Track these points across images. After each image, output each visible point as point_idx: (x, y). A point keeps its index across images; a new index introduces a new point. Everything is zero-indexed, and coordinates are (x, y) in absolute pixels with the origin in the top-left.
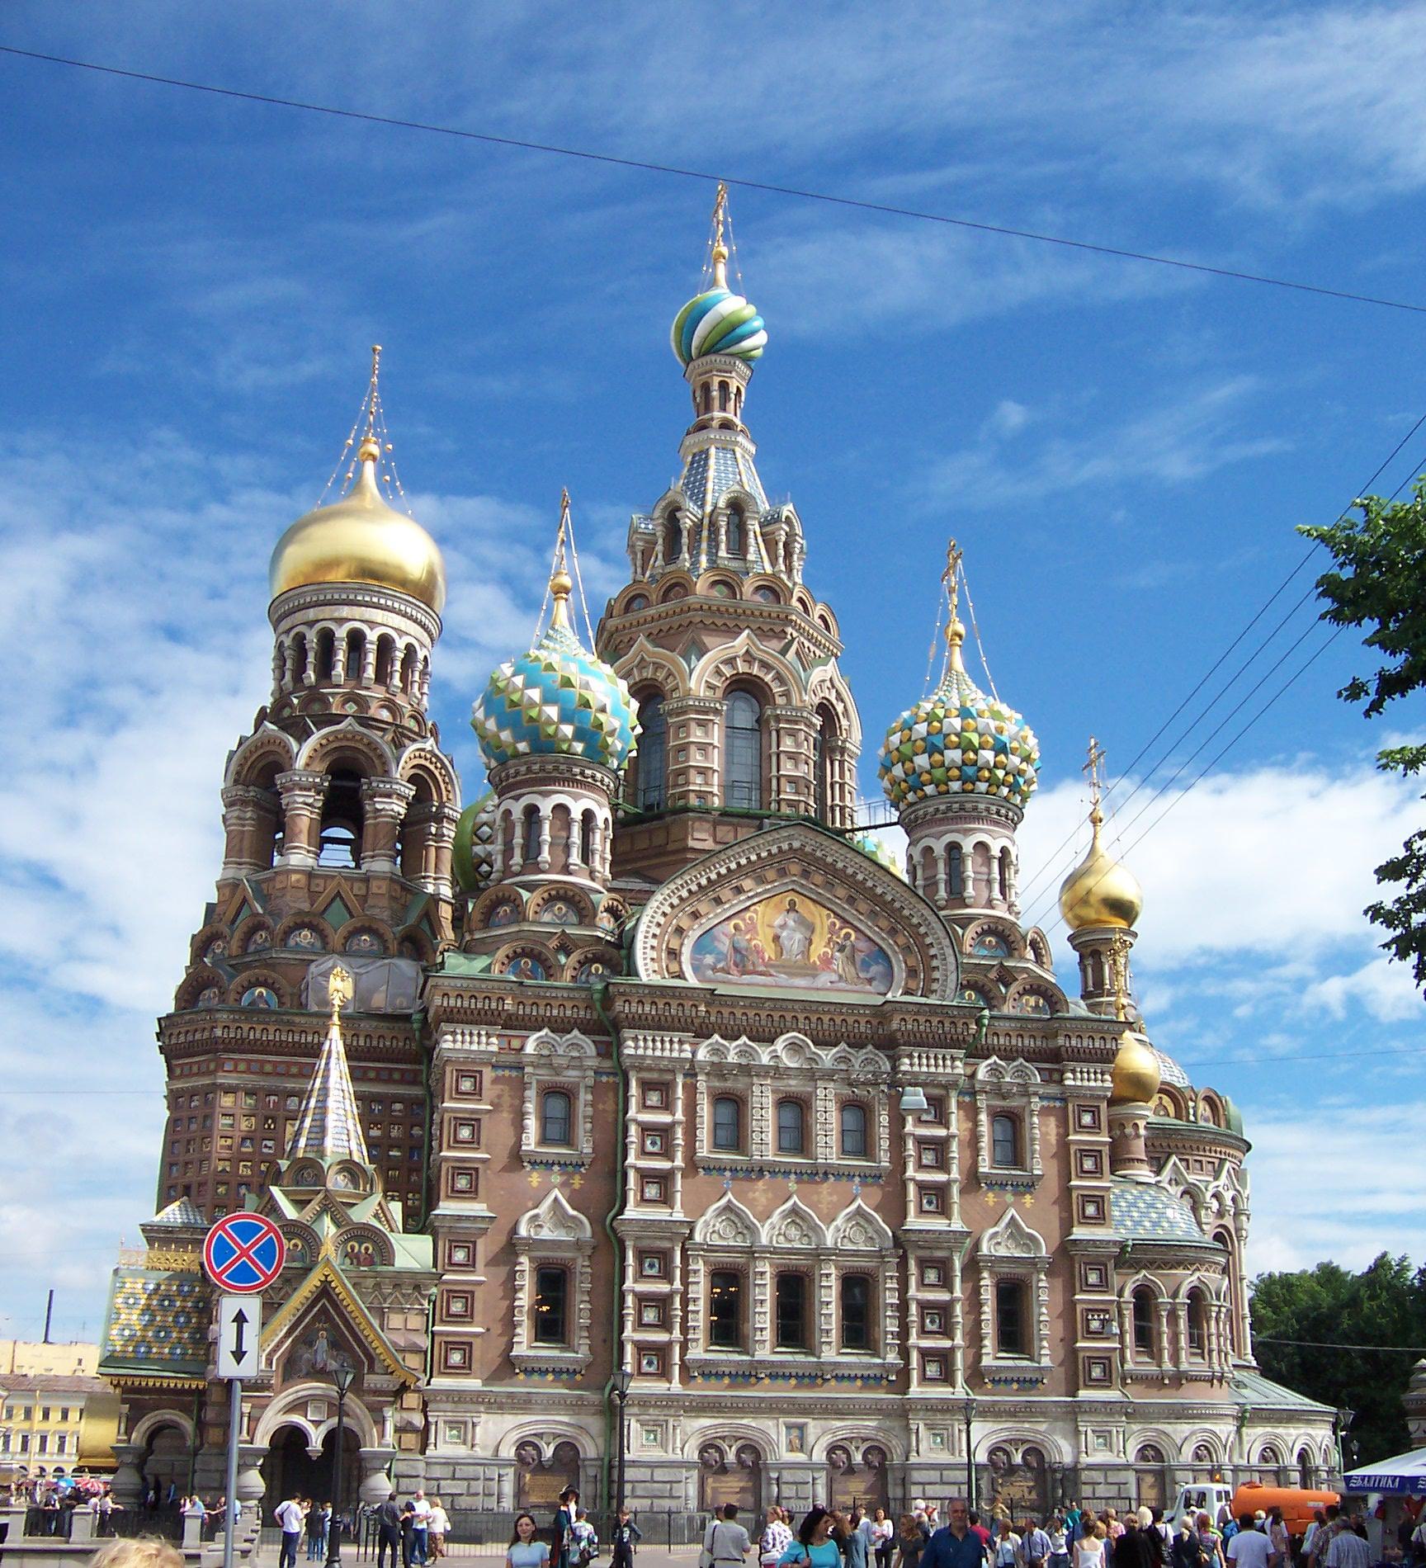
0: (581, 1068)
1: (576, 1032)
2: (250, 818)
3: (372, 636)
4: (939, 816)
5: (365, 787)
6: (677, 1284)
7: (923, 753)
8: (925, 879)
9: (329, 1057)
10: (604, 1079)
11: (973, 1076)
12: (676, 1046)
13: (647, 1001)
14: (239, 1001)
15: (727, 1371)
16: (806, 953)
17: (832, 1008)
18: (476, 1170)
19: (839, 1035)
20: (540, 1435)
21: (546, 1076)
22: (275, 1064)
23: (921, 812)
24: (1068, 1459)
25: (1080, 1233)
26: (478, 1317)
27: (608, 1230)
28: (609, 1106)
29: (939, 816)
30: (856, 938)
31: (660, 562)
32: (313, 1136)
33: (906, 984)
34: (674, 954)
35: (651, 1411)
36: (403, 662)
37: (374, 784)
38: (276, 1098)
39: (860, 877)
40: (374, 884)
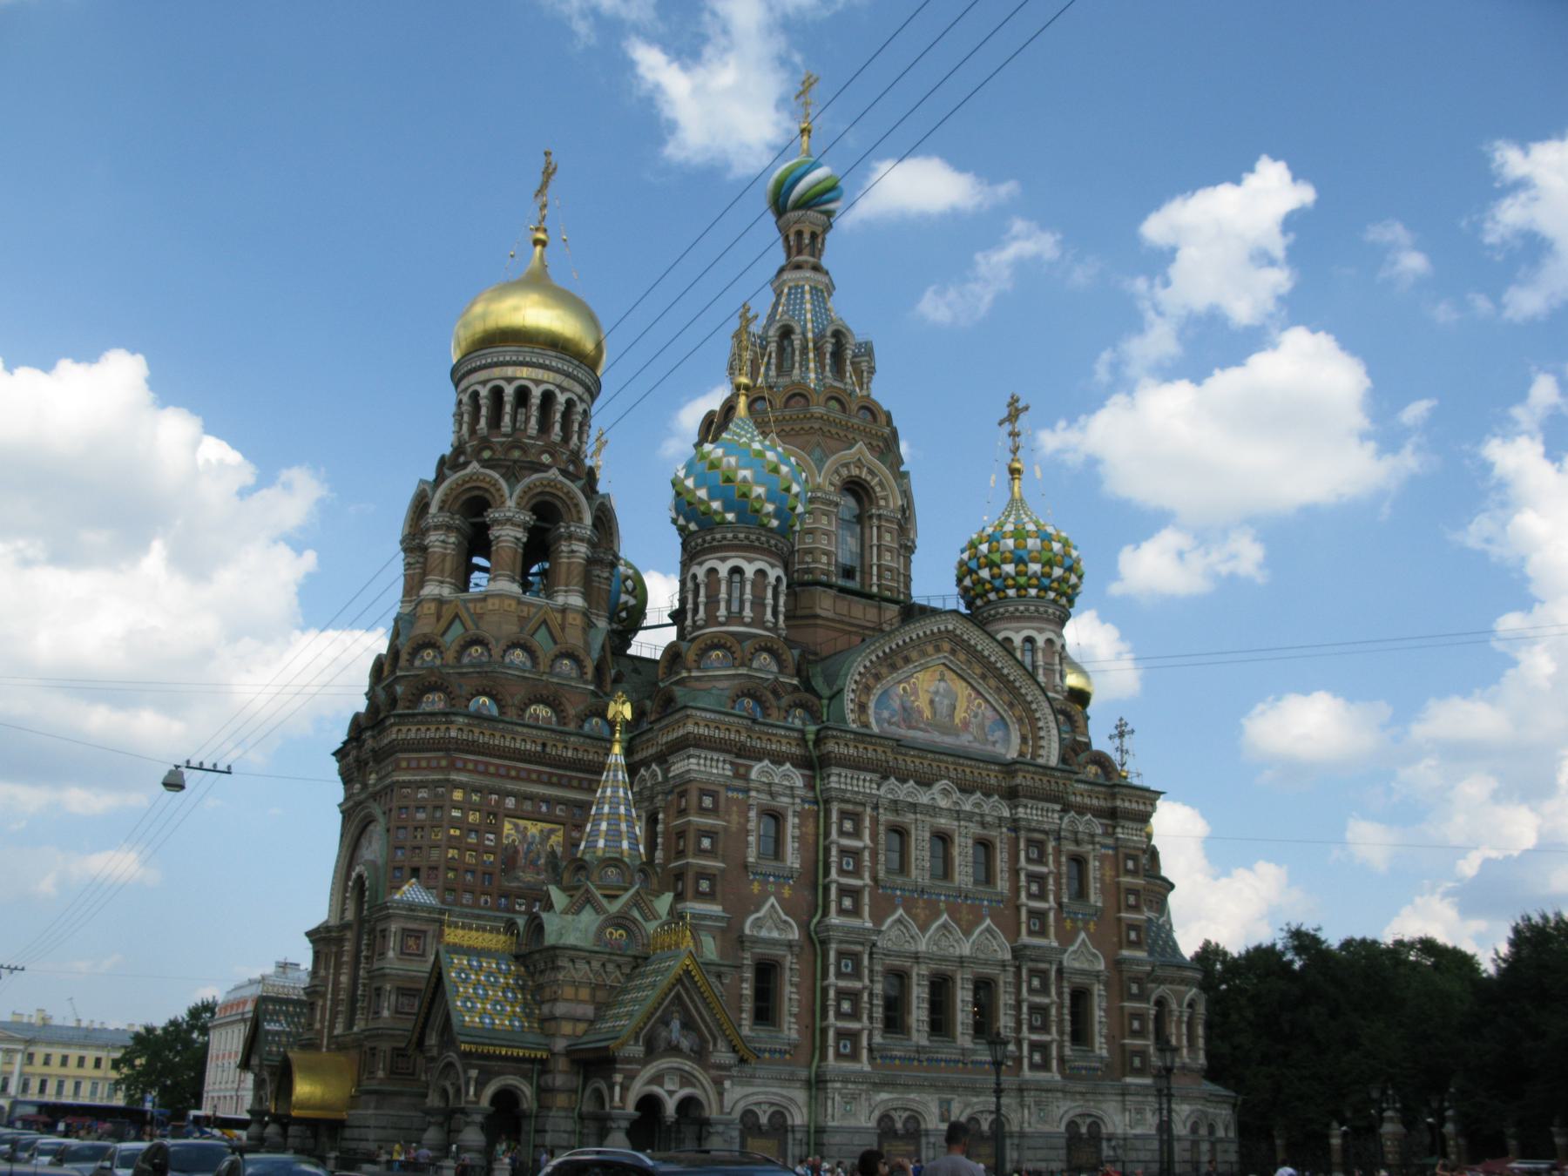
0: (793, 797)
1: (788, 765)
2: (454, 543)
3: (561, 398)
4: (1018, 614)
5: (562, 530)
6: (867, 981)
7: (1011, 562)
9: (616, 771)
10: (806, 806)
12: (867, 784)
13: (851, 744)
14: (467, 707)
15: (898, 1054)
16: (951, 715)
17: (973, 763)
18: (714, 875)
20: (759, 1104)
21: (765, 798)
22: (498, 766)
24: (1119, 1131)
25: (1126, 953)
28: (810, 829)
31: (773, 373)
32: (610, 838)
34: (862, 708)
35: (850, 1086)
36: (581, 425)
37: (573, 529)
38: (496, 797)
40: (570, 617)
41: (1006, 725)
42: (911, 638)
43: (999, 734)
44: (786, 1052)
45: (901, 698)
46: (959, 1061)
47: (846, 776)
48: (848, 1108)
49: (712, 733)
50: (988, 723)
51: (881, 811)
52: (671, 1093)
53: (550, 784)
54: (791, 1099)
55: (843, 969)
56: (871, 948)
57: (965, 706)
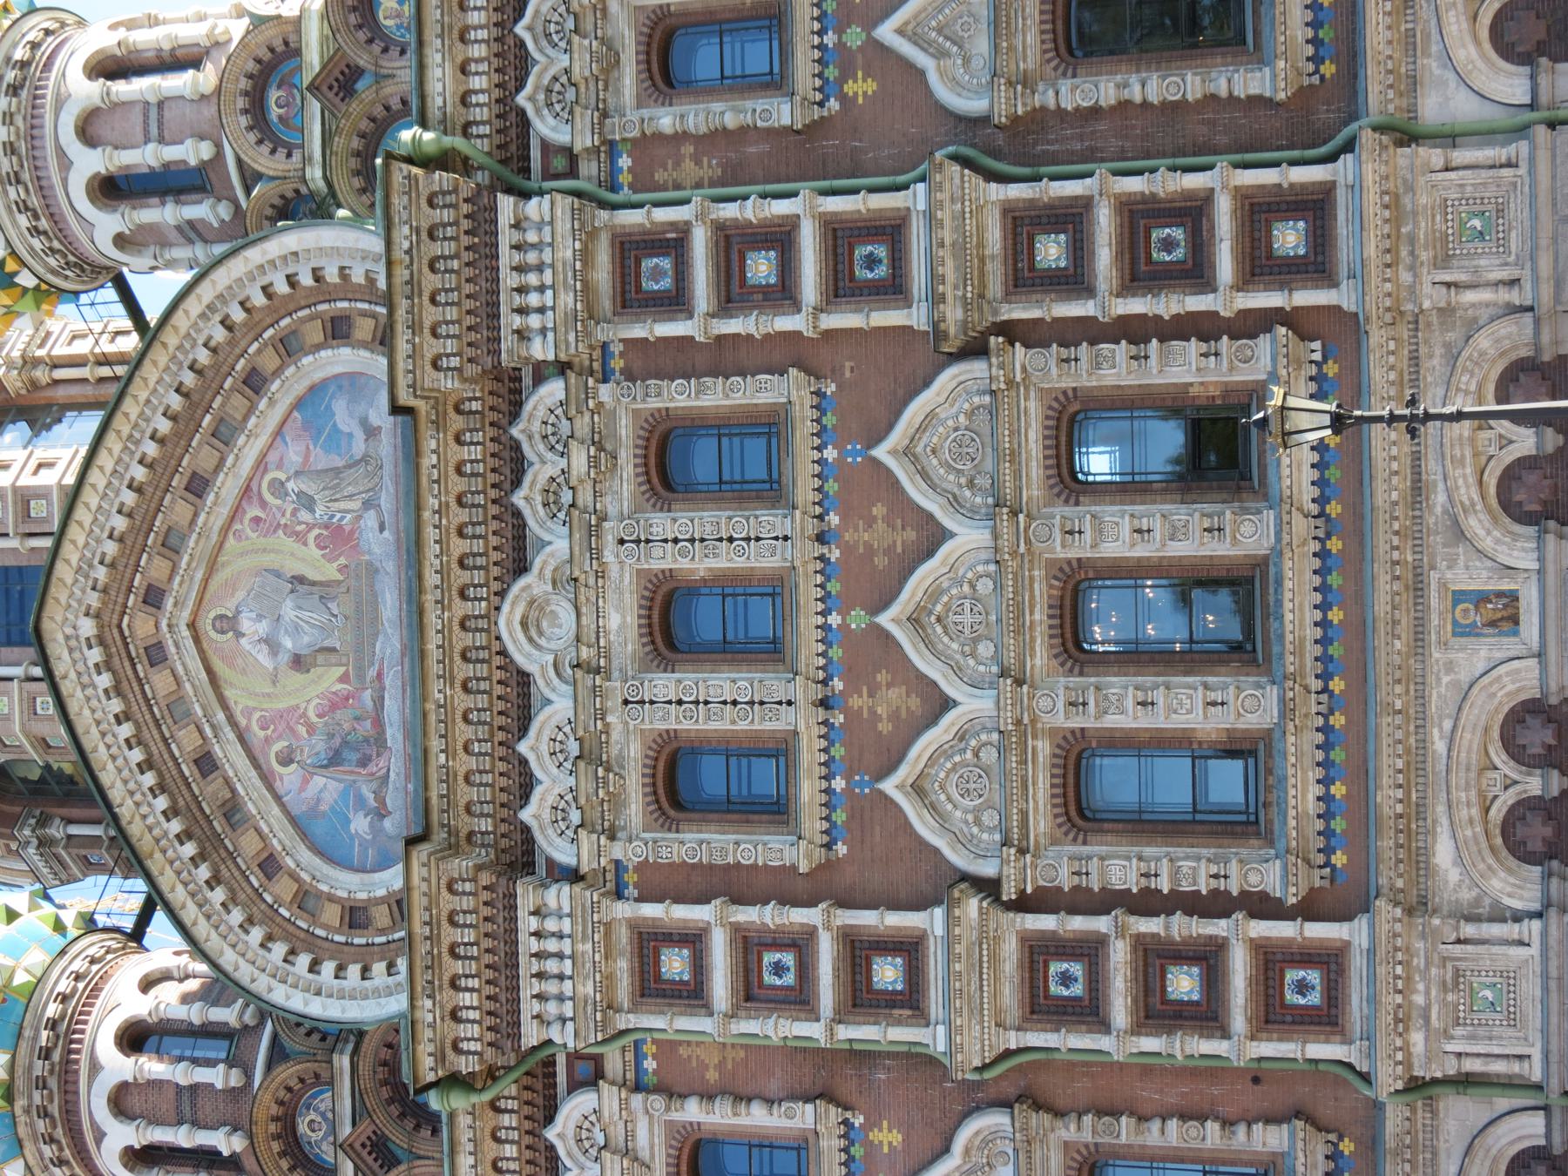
1: (551, 1134)
4: (44, 224)
6: (1102, 924)
8: (191, 242)
10: (650, 1064)
11: (569, 152)
12: (551, 925)
17: (431, 534)
19: (494, 510)
23: (52, 261)
27: (987, 1075)
29: (44, 224)
30: (279, 467)
33: (364, 345)
34: (355, 916)
35: (1419, 999)
39: (140, 473)
41: (312, 389)
42: (145, 766)
43: (343, 415)
45: (309, 772)
47: (540, 997)
48: (1488, 994)
50: (321, 460)
51: (617, 851)
55: (1077, 990)
57: (289, 543)
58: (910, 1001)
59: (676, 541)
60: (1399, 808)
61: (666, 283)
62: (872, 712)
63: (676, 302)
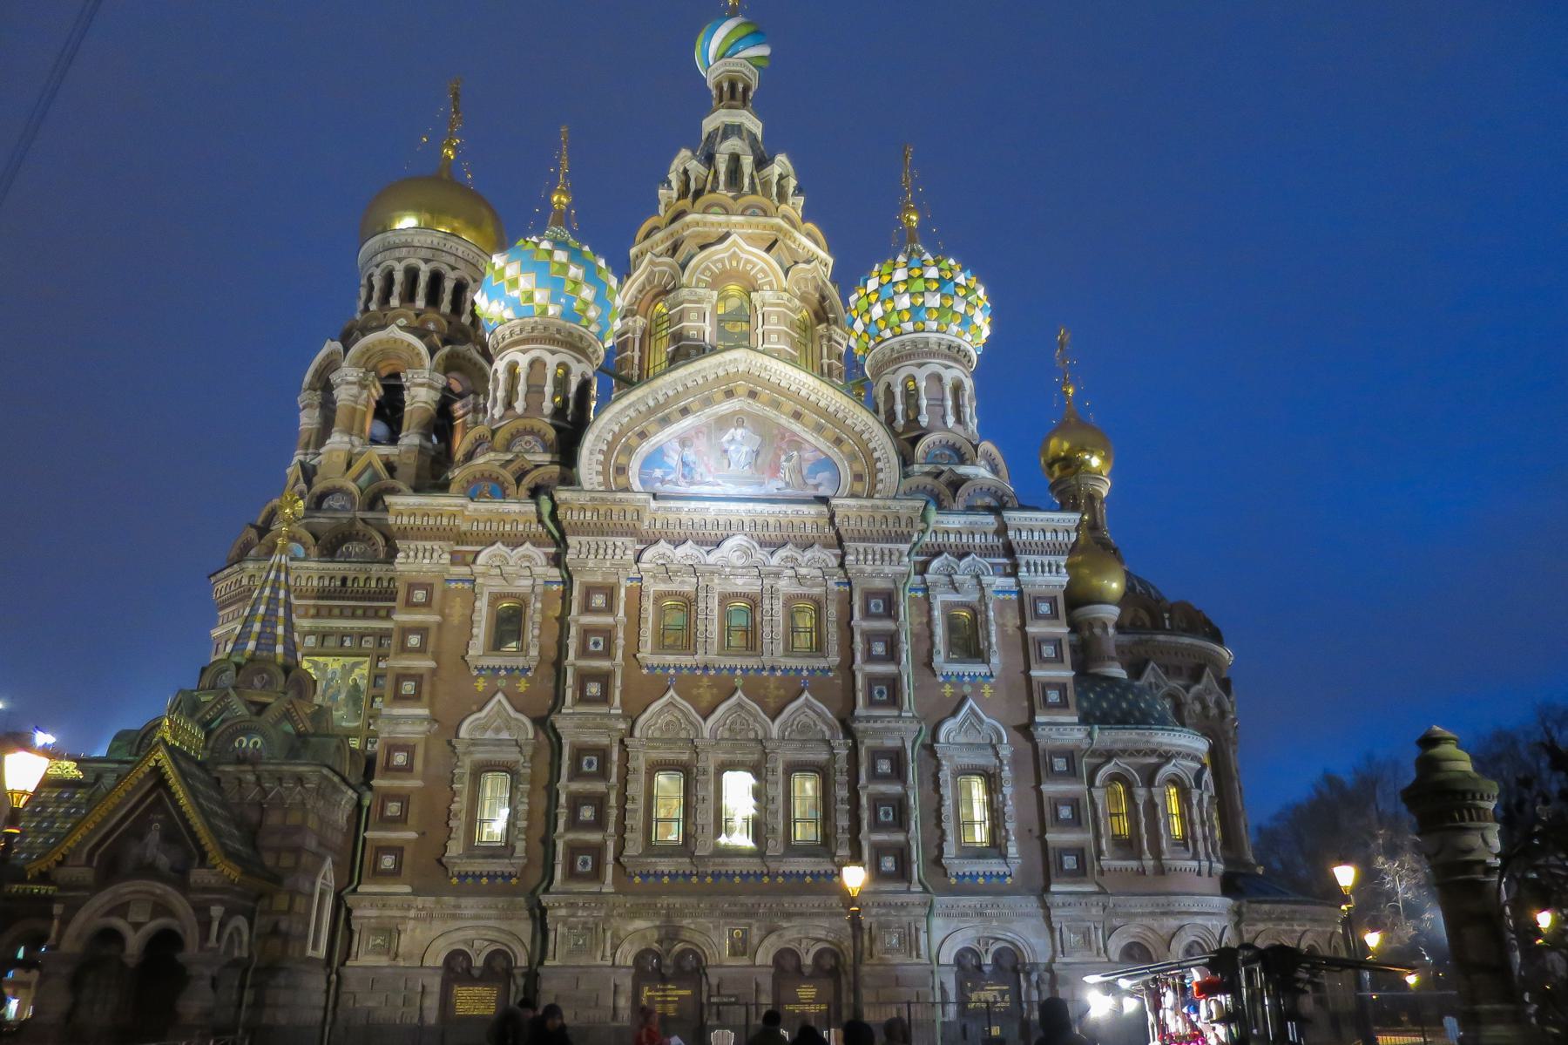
1: (528, 545)
5: (404, 380)
6: (614, 779)
18: (421, 676)
26: (412, 820)
34: (621, 470)
35: (580, 913)
43: (823, 476)
44: (510, 876)
46: (762, 874)
48: (581, 942)
49: (418, 522)
52: (137, 926)
53: (354, 616)
54: (512, 934)
55: (585, 768)
56: (622, 741)
58: (583, 699)
59: (772, 609)
60: (659, 905)
61: (873, 609)
62: (701, 686)
63: (867, 614)
